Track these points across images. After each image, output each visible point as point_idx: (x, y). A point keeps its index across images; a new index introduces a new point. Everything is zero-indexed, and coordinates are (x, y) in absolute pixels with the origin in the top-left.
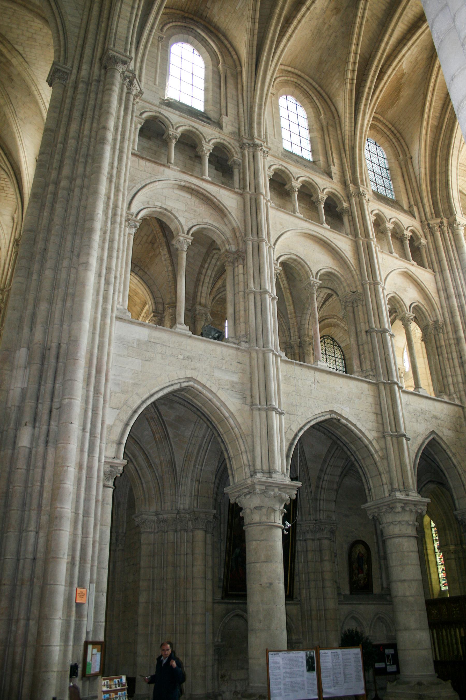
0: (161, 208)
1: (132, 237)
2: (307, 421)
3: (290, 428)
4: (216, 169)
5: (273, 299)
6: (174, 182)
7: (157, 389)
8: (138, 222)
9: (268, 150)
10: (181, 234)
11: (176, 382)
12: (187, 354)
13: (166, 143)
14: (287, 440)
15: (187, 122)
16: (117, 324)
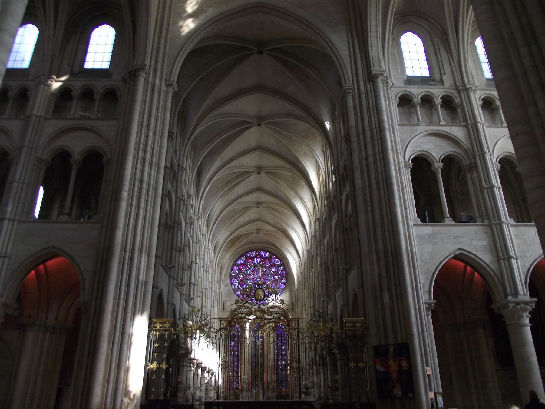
0: (421, 151)
1: (410, 174)
2: (535, 259)
3: (523, 266)
4: (446, 110)
5: (499, 188)
6: (424, 133)
7: (442, 259)
8: (410, 165)
9: (476, 88)
10: (436, 163)
11: (452, 252)
12: (455, 235)
13: (414, 106)
14: (523, 273)
15: (423, 90)
16: (414, 228)
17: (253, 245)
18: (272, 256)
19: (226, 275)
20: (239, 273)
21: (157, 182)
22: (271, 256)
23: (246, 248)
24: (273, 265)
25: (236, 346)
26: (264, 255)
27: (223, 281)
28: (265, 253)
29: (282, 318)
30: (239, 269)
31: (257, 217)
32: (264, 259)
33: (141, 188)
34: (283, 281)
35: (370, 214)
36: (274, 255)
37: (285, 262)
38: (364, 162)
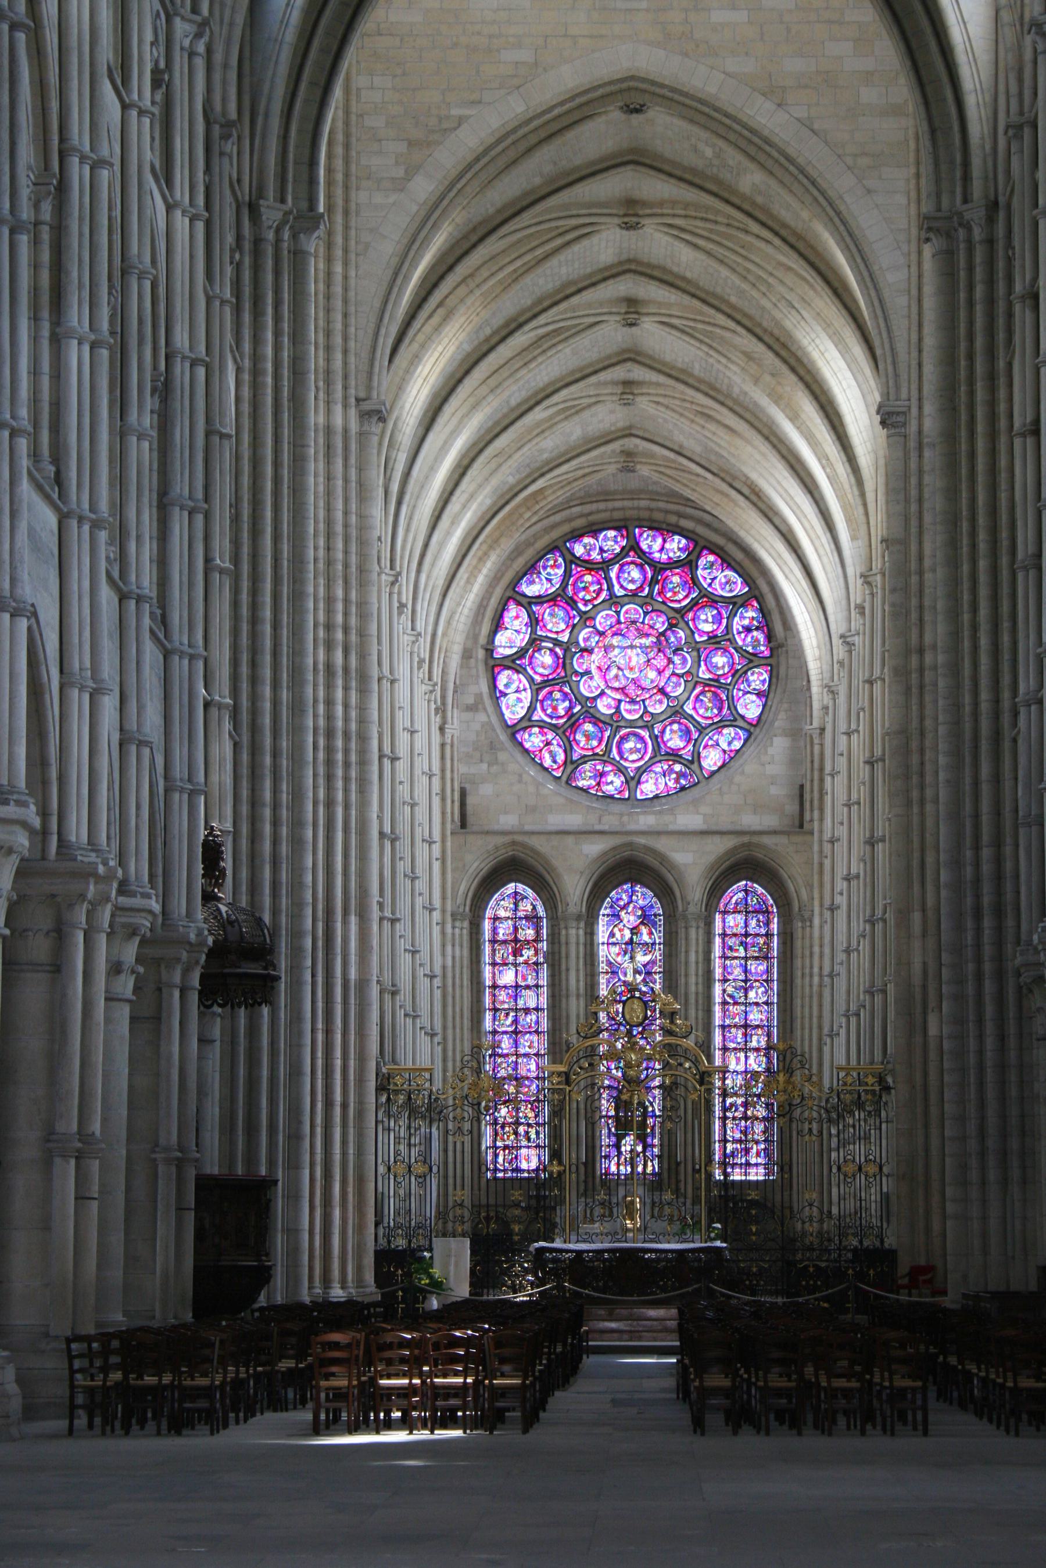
17: (602, 506)
18: (699, 557)
19: (467, 655)
20: (535, 643)
21: (362, 721)
22: (693, 557)
23: (570, 520)
24: (713, 601)
25: (528, 987)
26: (662, 550)
27: (455, 692)
28: (664, 541)
29: (687, 1065)
30: (535, 621)
31: (620, 424)
32: (659, 570)
33: (330, 750)
34: (758, 678)
35: (916, 809)
36: (712, 552)
37: (764, 588)
38: (914, 660)
